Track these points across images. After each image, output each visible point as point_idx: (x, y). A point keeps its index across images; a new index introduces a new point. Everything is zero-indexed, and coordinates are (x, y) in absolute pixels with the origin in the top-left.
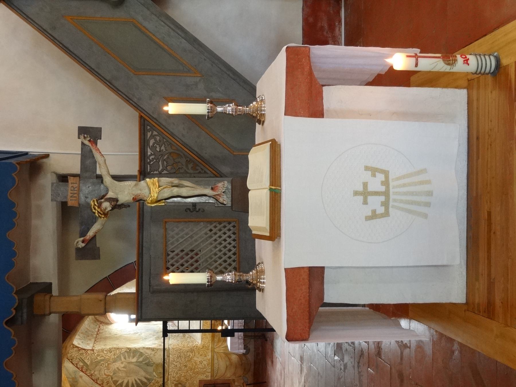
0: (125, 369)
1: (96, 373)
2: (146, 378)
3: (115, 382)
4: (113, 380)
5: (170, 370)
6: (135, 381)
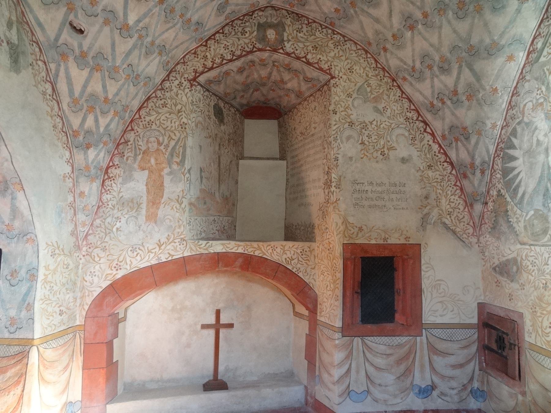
0: (535, 145)
1: (527, 85)
2: (524, 194)
3: (514, 133)
4: (517, 127)
5: (538, 248)
6: (519, 173)
